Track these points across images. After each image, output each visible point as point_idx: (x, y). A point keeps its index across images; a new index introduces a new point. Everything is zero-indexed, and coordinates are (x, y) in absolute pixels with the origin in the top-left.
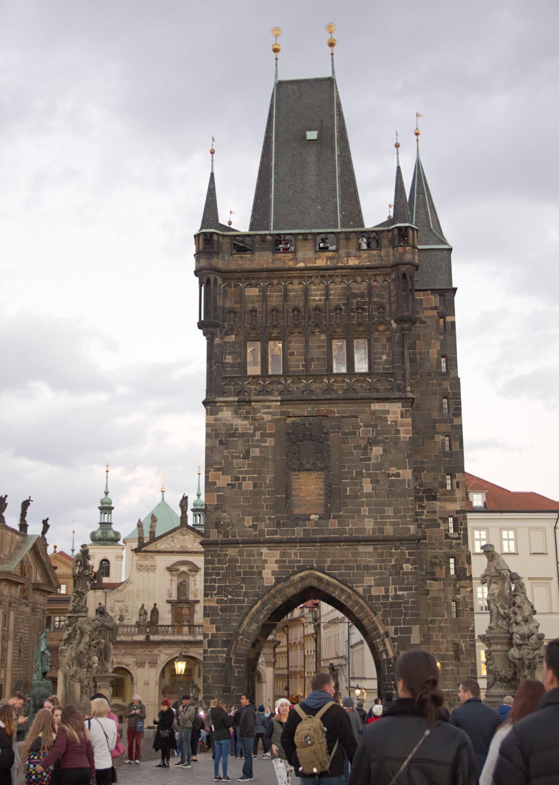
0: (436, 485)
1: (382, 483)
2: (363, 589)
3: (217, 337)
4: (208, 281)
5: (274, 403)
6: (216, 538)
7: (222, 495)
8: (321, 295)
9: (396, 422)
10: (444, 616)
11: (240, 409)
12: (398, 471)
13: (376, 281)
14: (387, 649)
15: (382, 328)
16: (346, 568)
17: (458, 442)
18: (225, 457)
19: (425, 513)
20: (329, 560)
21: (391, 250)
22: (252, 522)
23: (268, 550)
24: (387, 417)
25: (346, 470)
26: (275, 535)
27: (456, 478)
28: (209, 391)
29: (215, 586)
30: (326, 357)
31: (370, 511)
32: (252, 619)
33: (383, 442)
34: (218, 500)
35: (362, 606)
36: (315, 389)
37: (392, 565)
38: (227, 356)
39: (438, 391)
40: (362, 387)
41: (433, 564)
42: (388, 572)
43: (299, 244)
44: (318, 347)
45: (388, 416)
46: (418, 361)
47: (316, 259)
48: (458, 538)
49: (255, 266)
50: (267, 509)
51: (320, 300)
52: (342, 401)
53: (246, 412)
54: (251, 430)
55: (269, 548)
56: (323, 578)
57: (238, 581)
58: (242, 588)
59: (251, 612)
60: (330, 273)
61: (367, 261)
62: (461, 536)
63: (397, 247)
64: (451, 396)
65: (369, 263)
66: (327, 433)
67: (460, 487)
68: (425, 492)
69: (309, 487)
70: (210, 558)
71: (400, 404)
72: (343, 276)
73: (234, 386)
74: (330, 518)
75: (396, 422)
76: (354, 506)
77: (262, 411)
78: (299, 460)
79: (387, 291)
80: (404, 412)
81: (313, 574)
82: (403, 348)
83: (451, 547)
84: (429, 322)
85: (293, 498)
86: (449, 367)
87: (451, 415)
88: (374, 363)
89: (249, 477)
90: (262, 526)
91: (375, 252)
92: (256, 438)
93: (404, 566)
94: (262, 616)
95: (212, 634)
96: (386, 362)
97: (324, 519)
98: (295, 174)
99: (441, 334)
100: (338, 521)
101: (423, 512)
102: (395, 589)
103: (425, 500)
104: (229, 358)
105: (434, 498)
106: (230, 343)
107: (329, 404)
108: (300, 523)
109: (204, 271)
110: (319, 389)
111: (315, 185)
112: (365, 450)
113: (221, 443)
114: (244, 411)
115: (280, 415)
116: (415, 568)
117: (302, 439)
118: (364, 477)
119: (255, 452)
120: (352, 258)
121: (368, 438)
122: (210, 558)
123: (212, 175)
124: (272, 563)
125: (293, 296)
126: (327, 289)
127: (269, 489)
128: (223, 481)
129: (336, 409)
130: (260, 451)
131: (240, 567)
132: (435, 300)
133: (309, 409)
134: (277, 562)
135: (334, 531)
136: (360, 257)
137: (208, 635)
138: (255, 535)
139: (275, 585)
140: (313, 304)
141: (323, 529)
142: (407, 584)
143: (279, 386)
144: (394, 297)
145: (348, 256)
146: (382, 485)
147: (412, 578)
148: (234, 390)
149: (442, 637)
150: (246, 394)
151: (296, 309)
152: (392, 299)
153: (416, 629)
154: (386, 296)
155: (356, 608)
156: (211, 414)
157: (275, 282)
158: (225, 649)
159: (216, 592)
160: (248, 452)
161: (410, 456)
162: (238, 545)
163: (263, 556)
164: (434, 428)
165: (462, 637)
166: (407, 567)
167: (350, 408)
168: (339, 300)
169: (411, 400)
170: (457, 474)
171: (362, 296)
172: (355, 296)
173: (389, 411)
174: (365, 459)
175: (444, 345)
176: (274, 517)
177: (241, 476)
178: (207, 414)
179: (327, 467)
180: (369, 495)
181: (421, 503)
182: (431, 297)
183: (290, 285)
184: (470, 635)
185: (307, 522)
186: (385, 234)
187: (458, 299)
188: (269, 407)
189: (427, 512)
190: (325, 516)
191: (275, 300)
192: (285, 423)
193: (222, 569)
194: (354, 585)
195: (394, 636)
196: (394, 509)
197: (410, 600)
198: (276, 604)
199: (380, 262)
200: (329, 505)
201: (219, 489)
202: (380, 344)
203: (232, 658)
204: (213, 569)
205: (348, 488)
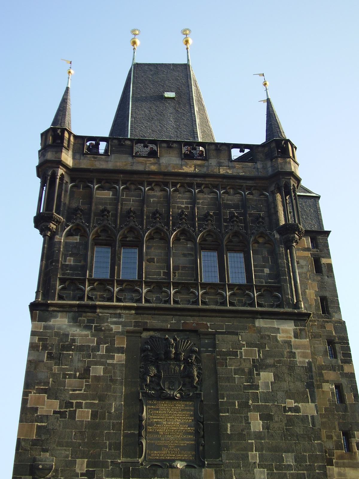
1: (276, 419)
8: (186, 203)
9: (289, 343)
11: (81, 317)
15: (261, 240)
18: (54, 375)
22: (87, 467)
24: (276, 337)
27: (355, 437)
33: (274, 366)
47: (182, 165)
51: (187, 208)
53: (87, 320)
60: (199, 180)
61: (241, 171)
74: (202, 466)
76: (238, 450)
77: (109, 320)
80: (298, 331)
89: (86, 403)
91: (250, 164)
92: (99, 353)
96: (269, 276)
97: (195, 468)
100: (216, 472)
104: (70, 260)
107: (199, 316)
108: (159, 471)
113: (50, 356)
115: (135, 326)
128: (49, 406)
129: (209, 324)
130: (105, 370)
133: (174, 322)
143: (134, 295)
145: (220, 165)
146: (276, 422)
164: (321, 375)
170: (355, 432)
171: (236, 207)
172: (228, 206)
174: (251, 387)
176: (119, 461)
180: (258, 436)
183: (150, 191)
185: (170, 470)
186: (260, 149)
188: (119, 316)
200: (201, 448)
201: (41, 419)
205: (229, 425)
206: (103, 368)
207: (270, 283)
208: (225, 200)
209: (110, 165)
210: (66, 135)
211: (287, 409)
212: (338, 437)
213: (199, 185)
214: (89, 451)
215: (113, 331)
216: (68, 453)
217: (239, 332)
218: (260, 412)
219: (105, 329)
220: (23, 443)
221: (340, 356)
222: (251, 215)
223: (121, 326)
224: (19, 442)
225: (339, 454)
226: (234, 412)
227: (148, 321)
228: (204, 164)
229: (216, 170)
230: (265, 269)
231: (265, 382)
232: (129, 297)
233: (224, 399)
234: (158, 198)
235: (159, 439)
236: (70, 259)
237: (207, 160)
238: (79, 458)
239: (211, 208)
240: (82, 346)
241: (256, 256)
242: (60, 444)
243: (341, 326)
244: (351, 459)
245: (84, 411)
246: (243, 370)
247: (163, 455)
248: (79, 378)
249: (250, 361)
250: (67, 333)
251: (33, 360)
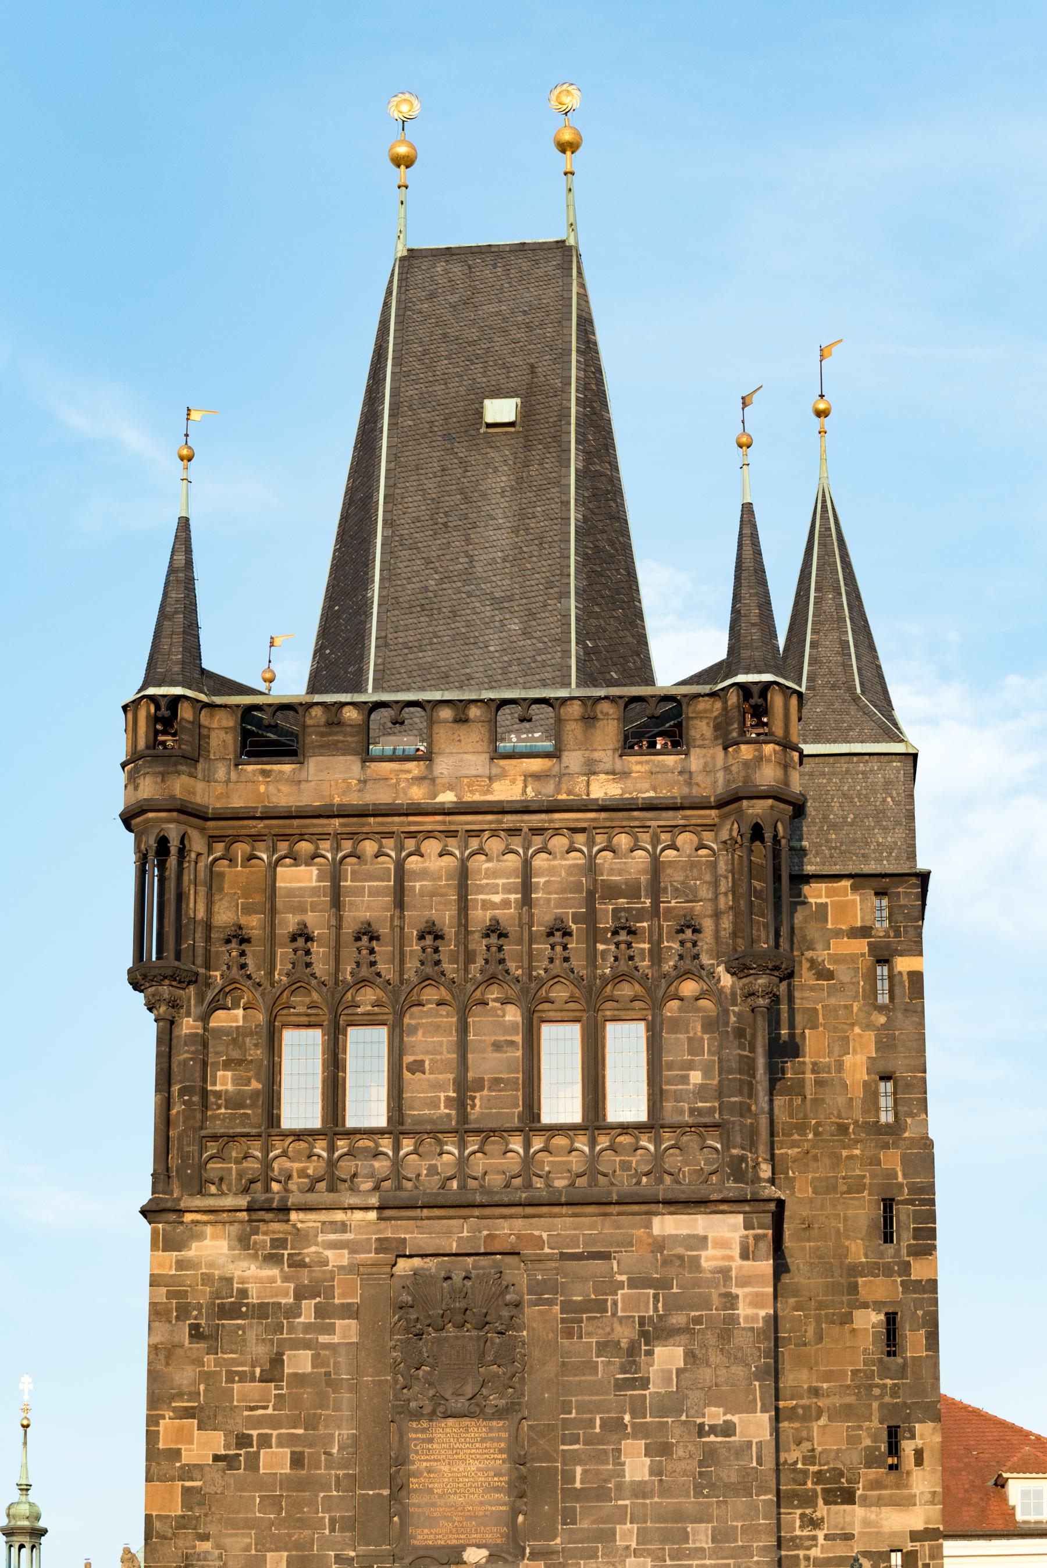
1: (679, 1452)
3: (188, 1015)
5: (359, 1215)
8: (507, 890)
9: (725, 1273)
12: (728, 1417)
13: (673, 846)
15: (689, 988)
17: (922, 1332)
18: (207, 1377)
19: (821, 1540)
21: (720, 753)
24: (698, 1257)
25: (573, 1415)
27: (913, 1437)
28: (161, 1177)
30: (520, 1075)
31: (643, 1537)
33: (686, 1330)
34: (186, 1505)
36: (485, 1173)
38: (219, 1073)
39: (867, 1181)
40: (625, 1166)
43: (442, 734)
44: (497, 1046)
45: (704, 1254)
46: (809, 1090)
49: (307, 798)
50: (332, 1530)
51: (506, 903)
52: (564, 1210)
54: (287, 1295)
60: (536, 820)
61: (647, 786)
63: (737, 744)
65: (652, 794)
66: (517, 1305)
67: (925, 1463)
68: (819, 1477)
69: (459, 1468)
71: (740, 1218)
72: (575, 830)
73: (238, 1162)
75: (725, 1273)
76: (594, 1522)
77: (320, 1239)
79: (708, 877)
80: (751, 1241)
82: (752, 1049)
85: (414, 1500)
87: (904, 1251)
89: (279, 1436)
91: (670, 760)
92: (302, 1319)
96: (701, 1092)
97: (505, 1561)
98: (445, 525)
101: (814, 1538)
103: (820, 1502)
105: (849, 1497)
106: (227, 1031)
109: (151, 815)
110: (498, 1172)
111: (504, 560)
112: (632, 1355)
113: (196, 1333)
114: (267, 1238)
118: (627, 1436)
119: (299, 1362)
120: (603, 776)
121: (642, 1319)
125: (422, 895)
126: (527, 871)
127: (341, 1473)
128: (202, 1446)
130: (315, 1358)
132: (859, 907)
133: (465, 1234)
136: (625, 774)
140: (480, 917)
143: (376, 1164)
144: (726, 894)
145: (590, 770)
148: (240, 1175)
150: (275, 1186)
151: (432, 933)
154: (705, 892)
157: (369, 847)
160: (277, 1361)
164: (854, 1289)
168: (562, 903)
169: (772, 1206)
170: (917, 1425)
171: (632, 891)
172: (613, 891)
173: (705, 1238)
174: (630, 1384)
176: (353, 1554)
177: (255, 1433)
178: (154, 1246)
180: (640, 1490)
181: (808, 1511)
182: (850, 897)
183: (414, 858)
186: (703, 705)
189: (827, 1537)
191: (368, 903)
199: (685, 790)
200: (521, 1518)
205: (579, 1470)
206: (312, 1355)
207: (700, 1112)
208: (605, 873)
211: (707, 1428)
212: (875, 1438)
214: (290, 1536)
215: (331, 1264)
216: (249, 1540)
217: (615, 1252)
218: (646, 1437)
219: (312, 1261)
220: (157, 1525)
221: (905, 1239)
223: (346, 1251)
224: (148, 1518)
225: (872, 1477)
227: (407, 1236)
228: (550, 770)
229: (580, 788)
230: (692, 1073)
231: (663, 1371)
232: (366, 1172)
233: (571, 1413)
234: (434, 880)
235: (433, 1505)
236: (224, 1076)
237: (559, 757)
238: (273, 1551)
239: (568, 899)
240: (263, 1306)
241: (673, 1036)
242: (234, 1524)
244: (898, 1487)
245: (276, 1454)
247: (440, 1537)
248: (261, 1381)
249: (634, 1322)
250: (227, 1275)
251: (162, 1343)
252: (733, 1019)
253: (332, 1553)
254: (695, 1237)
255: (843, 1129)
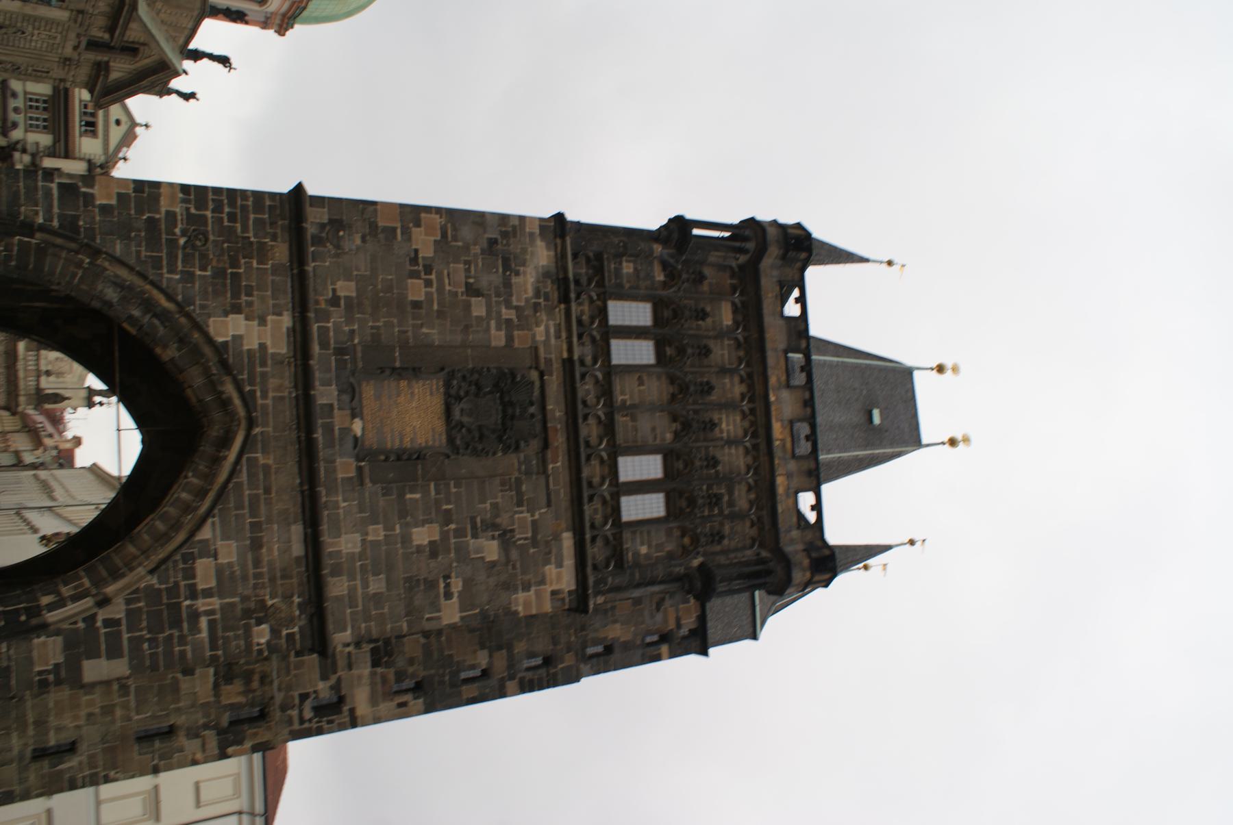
0: (400, 662)
1: (433, 564)
2: (207, 540)
4: (745, 239)
5: (565, 347)
6: (311, 218)
7: (395, 237)
8: (728, 431)
9: (542, 582)
10: (138, 714)
14: (65, 606)
15: (686, 540)
16: (254, 501)
18: (466, 248)
19: (348, 649)
20: (270, 462)
23: (288, 329)
26: (320, 344)
29: (206, 209)
31: (375, 544)
32: (131, 288)
33: (508, 561)
34: (385, 229)
35: (170, 539)
37: (263, 602)
40: (596, 511)
41: (248, 677)
42: (246, 593)
48: (302, 721)
50: (372, 327)
51: (722, 431)
54: (518, 300)
55: (292, 331)
56: (229, 449)
57: (218, 261)
58: (203, 268)
59: (148, 287)
60: (763, 447)
62: (306, 725)
63: (809, 556)
64: (552, 671)
70: (268, 203)
73: (587, 274)
77: (551, 323)
78: (467, 393)
79: (740, 545)
80: (561, 596)
81: (239, 425)
82: (661, 582)
83: (284, 708)
84: (659, 617)
86: (594, 660)
87: (519, 675)
88: (634, 533)
89: (431, 294)
90: (336, 317)
92: (504, 310)
93: (263, 626)
94: (136, 313)
95: (92, 196)
97: (355, 447)
99: (643, 640)
100: (351, 478)
102: (211, 612)
105: (376, 663)
108: (346, 398)
113: (493, 242)
116: (260, 652)
117: (507, 399)
118: (441, 526)
119: (478, 308)
122: (268, 203)
123: (866, 260)
124: (259, 338)
127: (410, 334)
128: (424, 242)
129: (558, 465)
130: (479, 318)
131: (249, 267)
132: (689, 622)
133: (558, 414)
134: (263, 347)
135: (332, 471)
136: (788, 496)
137: (92, 187)
138: (317, 302)
139: (210, 341)
141: (333, 446)
142: (223, 638)
145: (789, 476)
147: (238, 647)
149: (90, 715)
151: (708, 388)
152: (732, 555)
153: (120, 667)
155: (160, 526)
156: (541, 227)
158: (56, 223)
159: (193, 211)
161: (484, 615)
162: (295, 266)
163: (274, 317)
164: (500, 648)
165: (92, 757)
166: (262, 635)
167: (562, 492)
171: (731, 504)
172: (731, 492)
174: (474, 527)
175: (627, 646)
176: (356, 341)
177: (433, 277)
178: (541, 220)
179: (456, 450)
180: (406, 539)
184: (96, 774)
185: (348, 412)
187: (691, 661)
188: (558, 337)
189: (349, 653)
190: (362, 452)
191: (722, 353)
192: (530, 368)
193: (245, 228)
194: (216, 519)
195: (100, 618)
196: (381, 593)
197: (188, 648)
198: (165, 347)
202: (664, 539)
203: (32, 237)
204: (244, 208)
205: (418, 496)
209: (768, 319)
210: (803, 255)
213: (755, 447)
218: (442, 540)
220: (371, 208)
221: (529, 675)
222: (722, 524)
226: (437, 503)
243: (572, 677)
246: (497, 516)
248: (467, 284)
252: (677, 569)
253: (356, 327)
254: (562, 561)
255: (583, 628)
